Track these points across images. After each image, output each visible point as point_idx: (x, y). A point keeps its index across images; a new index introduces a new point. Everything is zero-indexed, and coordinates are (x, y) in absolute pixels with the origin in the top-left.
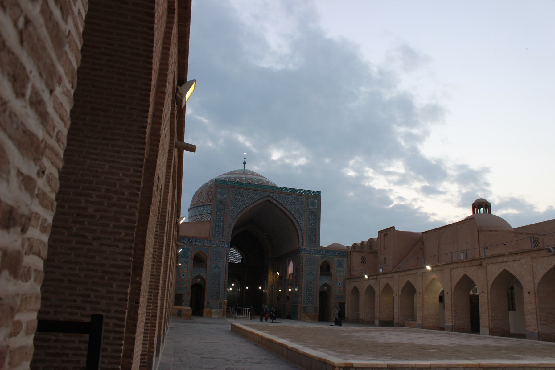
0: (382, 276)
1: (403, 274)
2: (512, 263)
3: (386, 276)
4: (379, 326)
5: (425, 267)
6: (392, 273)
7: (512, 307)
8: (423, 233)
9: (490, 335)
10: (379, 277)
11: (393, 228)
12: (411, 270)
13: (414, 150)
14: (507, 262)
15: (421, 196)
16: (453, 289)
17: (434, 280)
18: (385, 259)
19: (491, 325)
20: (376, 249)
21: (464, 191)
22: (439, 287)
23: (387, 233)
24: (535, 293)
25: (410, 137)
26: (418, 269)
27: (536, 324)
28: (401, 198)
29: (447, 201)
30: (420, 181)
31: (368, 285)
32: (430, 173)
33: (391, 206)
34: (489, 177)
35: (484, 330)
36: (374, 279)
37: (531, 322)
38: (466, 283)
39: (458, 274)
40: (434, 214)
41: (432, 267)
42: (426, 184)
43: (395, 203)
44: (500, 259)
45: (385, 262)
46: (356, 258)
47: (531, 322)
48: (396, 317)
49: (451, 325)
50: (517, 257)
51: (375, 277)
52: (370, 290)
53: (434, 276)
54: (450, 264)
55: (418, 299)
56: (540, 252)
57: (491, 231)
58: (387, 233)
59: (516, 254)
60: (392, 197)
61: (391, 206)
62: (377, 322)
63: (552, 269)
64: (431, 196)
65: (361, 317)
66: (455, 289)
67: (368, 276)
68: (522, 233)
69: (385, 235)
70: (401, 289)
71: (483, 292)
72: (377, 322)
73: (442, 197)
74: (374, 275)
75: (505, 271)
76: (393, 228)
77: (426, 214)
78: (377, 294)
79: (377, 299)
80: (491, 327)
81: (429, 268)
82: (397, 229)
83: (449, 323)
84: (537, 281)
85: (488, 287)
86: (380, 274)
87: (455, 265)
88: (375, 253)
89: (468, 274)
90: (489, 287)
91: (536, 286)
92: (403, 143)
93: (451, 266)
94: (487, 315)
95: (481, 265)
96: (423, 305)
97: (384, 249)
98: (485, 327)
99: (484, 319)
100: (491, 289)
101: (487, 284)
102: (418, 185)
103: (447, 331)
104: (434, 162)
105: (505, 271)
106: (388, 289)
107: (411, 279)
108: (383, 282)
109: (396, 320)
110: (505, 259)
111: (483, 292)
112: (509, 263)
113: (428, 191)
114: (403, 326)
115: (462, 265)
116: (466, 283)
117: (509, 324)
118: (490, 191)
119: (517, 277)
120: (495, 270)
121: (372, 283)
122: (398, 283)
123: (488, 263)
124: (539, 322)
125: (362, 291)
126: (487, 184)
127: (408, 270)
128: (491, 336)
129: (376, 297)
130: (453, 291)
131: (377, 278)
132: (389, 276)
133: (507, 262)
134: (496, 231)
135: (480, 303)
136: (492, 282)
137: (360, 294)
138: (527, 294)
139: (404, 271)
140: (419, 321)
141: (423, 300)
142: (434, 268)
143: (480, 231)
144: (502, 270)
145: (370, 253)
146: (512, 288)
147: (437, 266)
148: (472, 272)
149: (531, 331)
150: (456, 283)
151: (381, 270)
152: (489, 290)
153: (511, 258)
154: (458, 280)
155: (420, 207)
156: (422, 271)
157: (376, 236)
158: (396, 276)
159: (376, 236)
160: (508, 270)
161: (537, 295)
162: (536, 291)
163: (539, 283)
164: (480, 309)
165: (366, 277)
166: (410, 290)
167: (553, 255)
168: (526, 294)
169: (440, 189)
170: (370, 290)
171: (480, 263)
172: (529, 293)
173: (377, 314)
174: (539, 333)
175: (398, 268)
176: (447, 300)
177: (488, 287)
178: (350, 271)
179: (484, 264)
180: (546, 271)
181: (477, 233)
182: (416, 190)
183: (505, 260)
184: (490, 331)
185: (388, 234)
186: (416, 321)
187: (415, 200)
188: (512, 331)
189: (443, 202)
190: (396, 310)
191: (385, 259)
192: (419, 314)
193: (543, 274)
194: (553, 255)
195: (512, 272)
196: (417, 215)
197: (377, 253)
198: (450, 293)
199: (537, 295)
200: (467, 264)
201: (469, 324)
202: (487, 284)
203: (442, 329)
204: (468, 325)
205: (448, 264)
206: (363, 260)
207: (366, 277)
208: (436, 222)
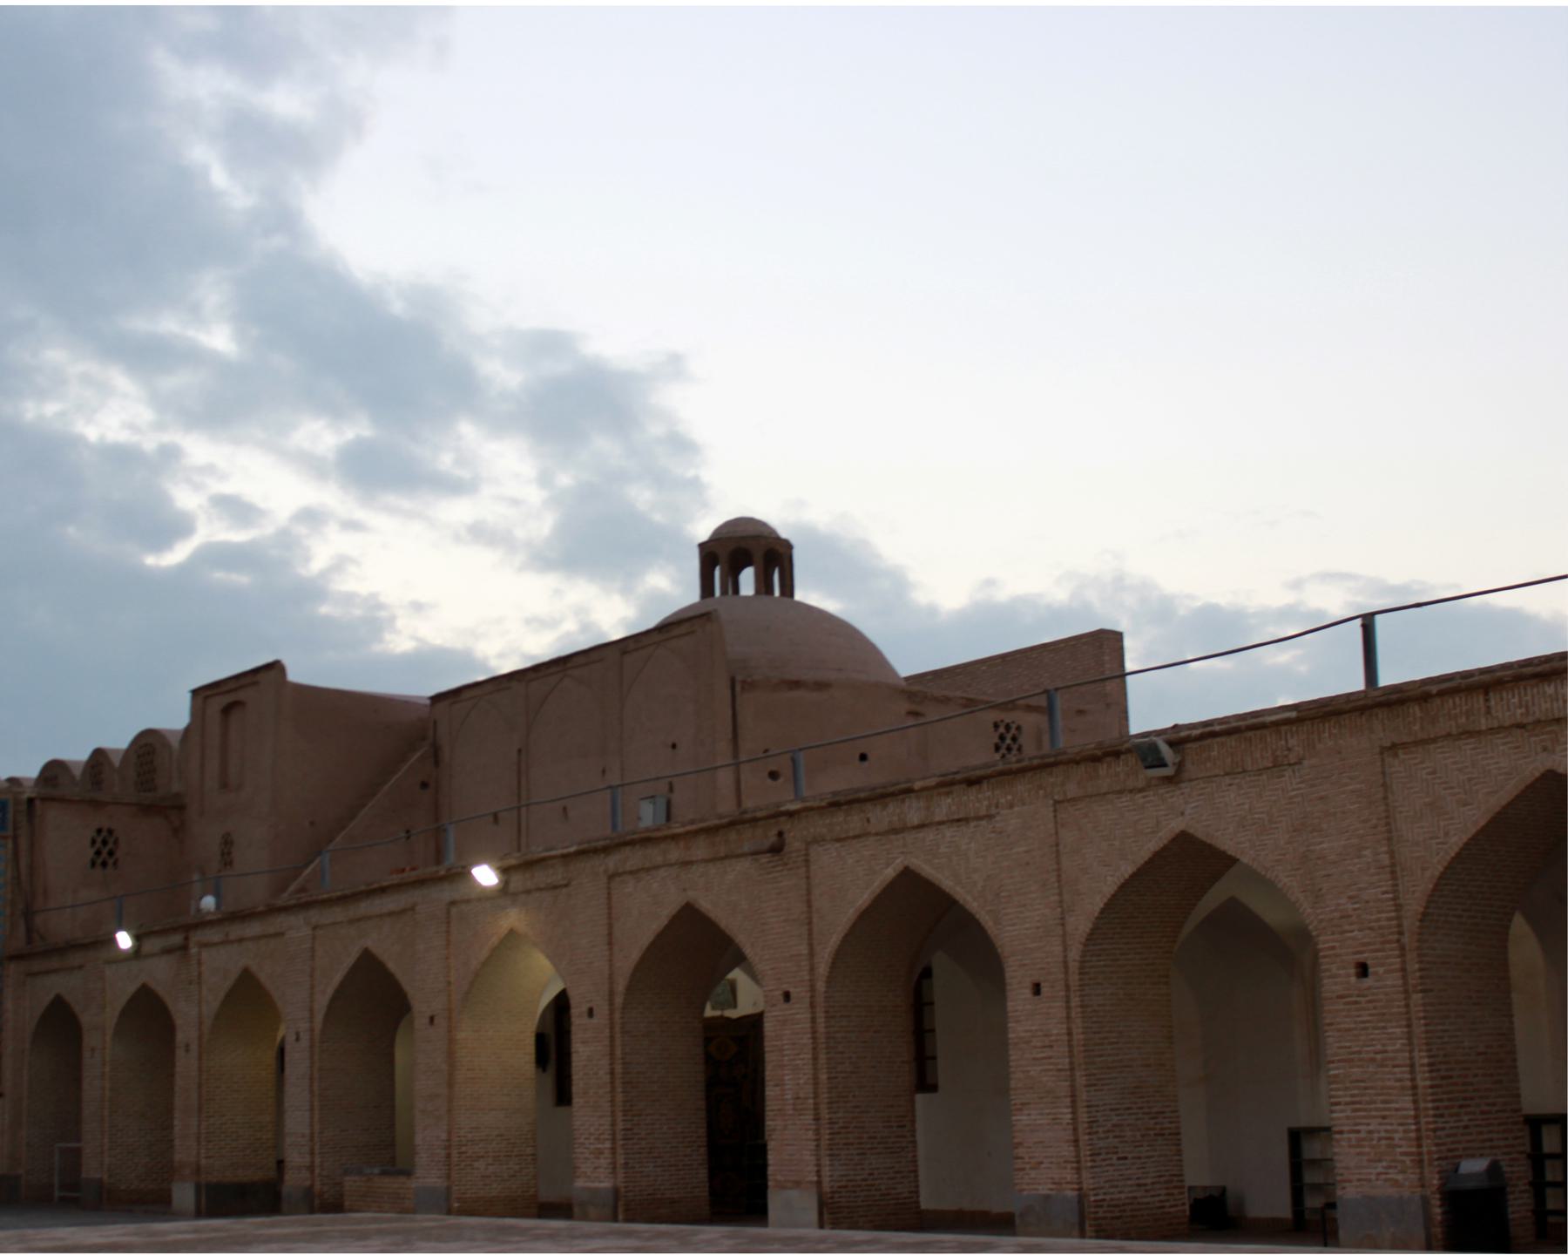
0: (213, 935)
1: (338, 914)
2: (949, 832)
3: (236, 930)
4: (199, 1214)
5: (464, 874)
6: (273, 910)
7: (925, 1082)
8: (437, 699)
9: (821, 1226)
10: (197, 936)
11: (275, 667)
12: (383, 890)
13: (282, 218)
14: (922, 826)
15: (331, 497)
16: (621, 986)
17: (510, 938)
18: (227, 842)
19: (826, 1171)
20: (176, 787)
21: (565, 480)
22: (539, 978)
23: (240, 696)
24: (1067, 987)
25: (253, 138)
26: (421, 882)
27: (1068, 1151)
28: (236, 509)
29: (480, 533)
30: (334, 412)
31: (132, 989)
32: (382, 373)
33: (177, 555)
34: (687, 406)
35: (790, 1200)
36: (168, 951)
37: (1044, 1141)
38: (696, 950)
39: (648, 907)
40: (418, 607)
41: (504, 871)
42: (359, 429)
43: (211, 531)
44: (881, 816)
45: (227, 860)
46: (65, 840)
47: (1044, 1141)
48: (296, 1157)
49: (606, 1184)
50: (977, 801)
51: (176, 939)
52: (148, 1016)
53: (513, 918)
54: (605, 850)
55: (417, 1056)
56: (1103, 769)
57: (796, 684)
58: (240, 696)
59: (972, 782)
60: (186, 499)
61: (177, 555)
62: (183, 1194)
63: (1157, 855)
64: (391, 499)
65: (92, 1169)
66: (630, 989)
67: (137, 938)
68: (946, 700)
69: (227, 710)
70: (322, 1001)
71: (787, 996)
72: (183, 1194)
73: (458, 511)
74: (170, 928)
75: (909, 879)
76: (275, 667)
77: (374, 604)
78: (186, 1033)
79: (186, 1064)
80: (826, 1187)
81: (485, 875)
82: (295, 675)
83: (594, 1175)
84: (1080, 924)
85: (812, 969)
86: (203, 923)
87: (633, 858)
88: (169, 810)
89: (705, 904)
90: (823, 969)
91: (1074, 954)
92: (219, 177)
93: (612, 862)
94: (808, 1118)
95: (777, 849)
96: (450, 1084)
97: (224, 785)
98: (798, 1184)
99: (792, 1145)
100: (830, 981)
101: (812, 954)
102: (321, 436)
103: (585, 1217)
104: (398, 307)
105: (909, 879)
106: (248, 999)
107: (384, 943)
108: (219, 964)
109: (294, 1180)
110: (913, 811)
111: (787, 996)
112: (930, 835)
113: (375, 472)
114: (335, 1206)
115: (675, 853)
116: (696, 950)
117: (914, 1161)
118: (695, 485)
119: (973, 905)
120: (852, 876)
121: (159, 973)
122: (303, 968)
123: (818, 840)
124: (1084, 1138)
125: (100, 1023)
126: (683, 445)
127: (370, 893)
128: (826, 1232)
129: (180, 1053)
130: (619, 1000)
131: (184, 948)
132: (254, 928)
133: (922, 826)
134: (822, 686)
135: (771, 1058)
136: (834, 940)
137: (90, 1040)
138: (1027, 993)
139: (344, 900)
140: (428, 1176)
141: (451, 1055)
142: (517, 881)
143: (739, 685)
144: (890, 873)
145: (147, 809)
146: (927, 973)
147: (529, 865)
148: (728, 892)
149: (1044, 1190)
150: (635, 955)
151: (209, 902)
152: (821, 986)
153: (944, 806)
154: (646, 937)
155: (340, 564)
156: (446, 893)
157: (174, 716)
158: (296, 927)
159: (174, 716)
160: (927, 870)
161: (1075, 1001)
162: (1074, 979)
163: (1091, 938)
164: (770, 1092)
165: (124, 940)
166: (375, 1003)
167: (1169, 780)
168: (1018, 998)
169: (446, 461)
170: (148, 1016)
171: (771, 838)
172: (1037, 989)
173: (185, 1151)
174: (1081, 1198)
175: (302, 890)
176: (587, 1051)
177: (812, 969)
178: (29, 914)
179: (794, 843)
180: (1127, 870)
181: (728, 693)
182: (311, 465)
183: (914, 818)
184: (822, 1205)
185: (245, 701)
186: (408, 1173)
187: (311, 517)
188: (926, 1203)
189: (457, 538)
190: (298, 1121)
191: (227, 842)
192: (427, 1137)
193: (1110, 886)
194: (1169, 780)
195: (946, 883)
196: (324, 610)
197: (181, 808)
198: (602, 1010)
199: (1075, 1001)
200: (700, 849)
201: (703, 1174)
202: (812, 954)
203: (560, 1209)
204: (698, 1178)
205: (595, 851)
206: (105, 851)
207: (124, 940)
208: (426, 658)
